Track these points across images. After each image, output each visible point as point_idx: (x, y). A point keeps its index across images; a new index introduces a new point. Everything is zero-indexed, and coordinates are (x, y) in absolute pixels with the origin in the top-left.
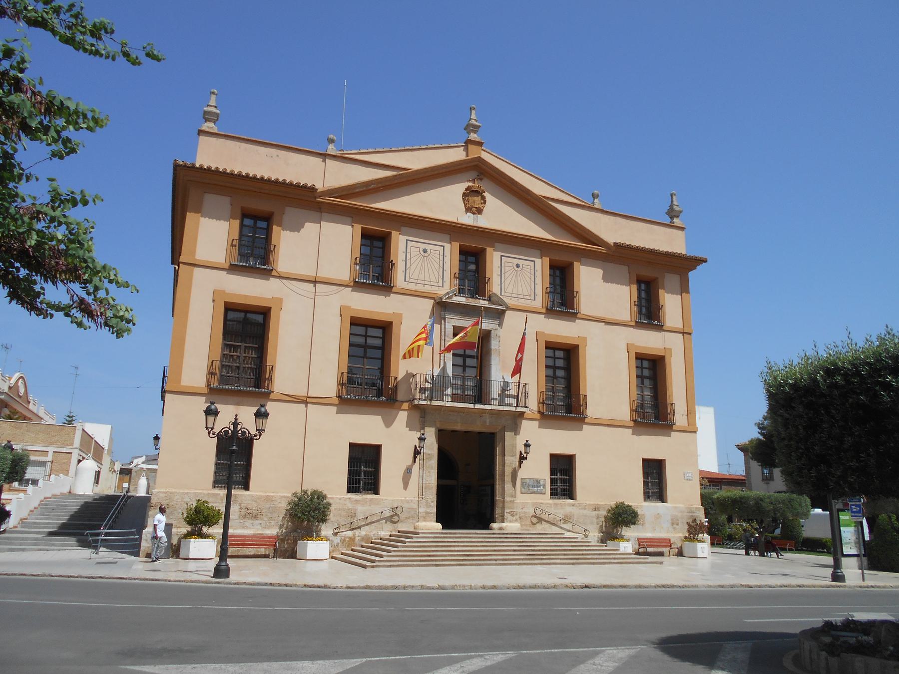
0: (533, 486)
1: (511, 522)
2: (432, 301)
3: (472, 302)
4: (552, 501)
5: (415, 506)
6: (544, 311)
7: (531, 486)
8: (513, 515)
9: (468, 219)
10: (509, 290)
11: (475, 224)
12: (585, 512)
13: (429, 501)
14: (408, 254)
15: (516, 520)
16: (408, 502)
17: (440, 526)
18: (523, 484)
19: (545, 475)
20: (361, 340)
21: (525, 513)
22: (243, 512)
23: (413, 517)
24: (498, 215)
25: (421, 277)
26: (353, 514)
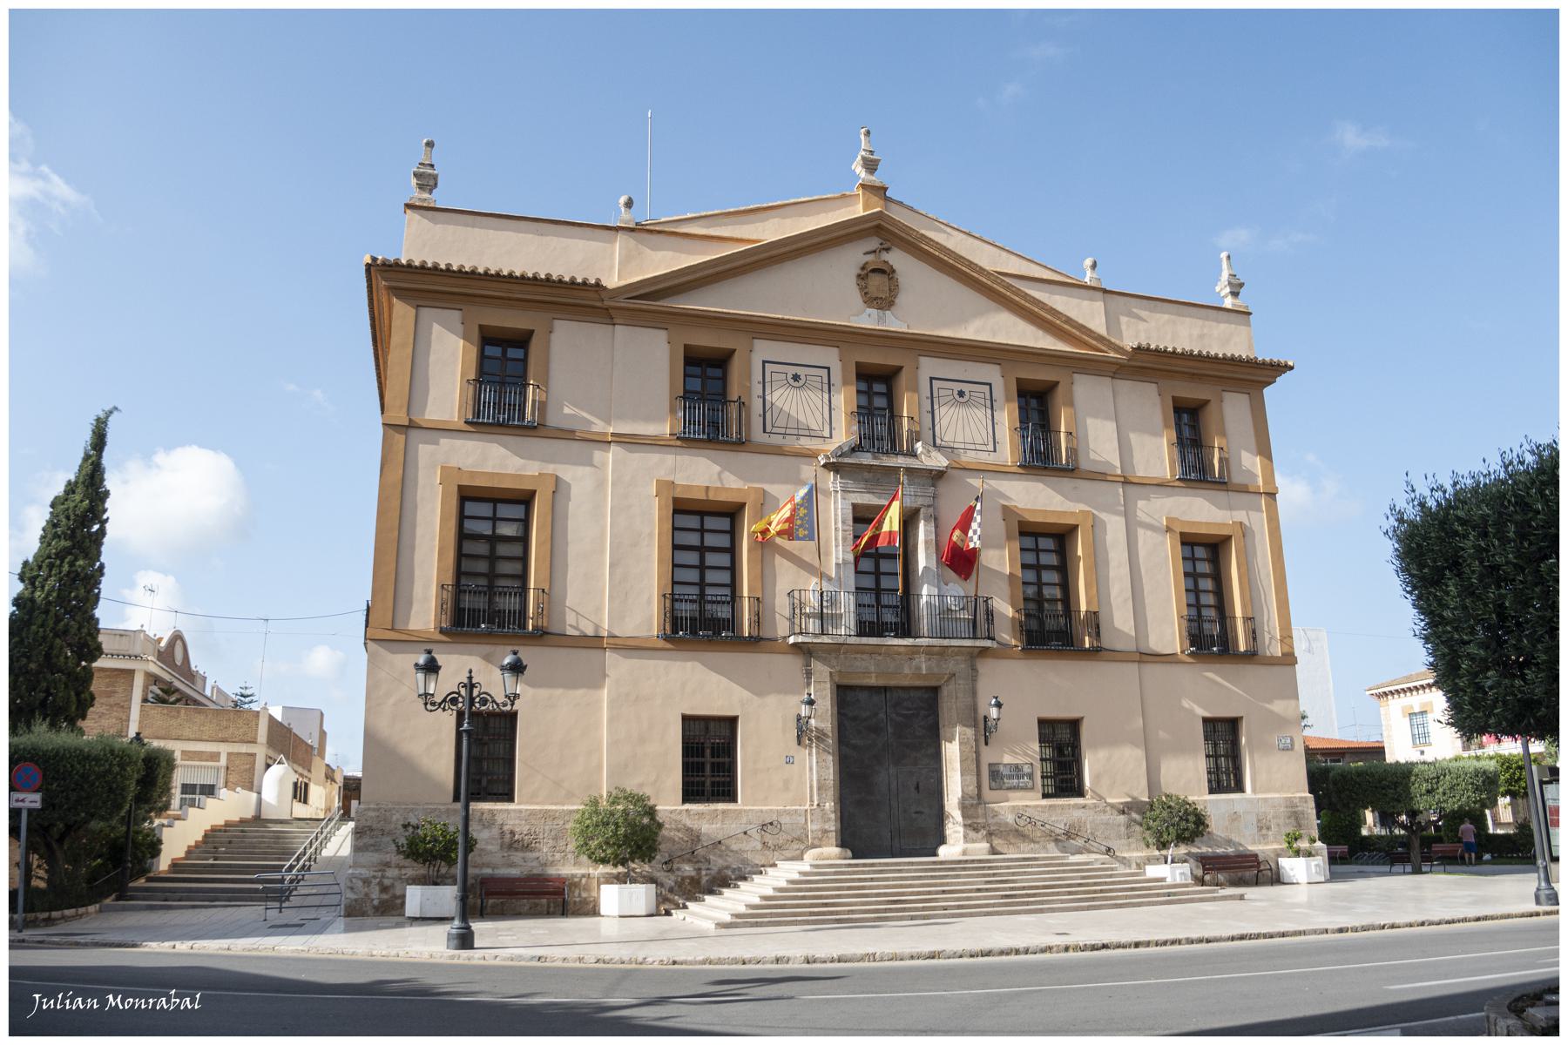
0: (1010, 777)
9: (868, 320)
12: (1105, 817)
20: (693, 539)
24: (926, 306)
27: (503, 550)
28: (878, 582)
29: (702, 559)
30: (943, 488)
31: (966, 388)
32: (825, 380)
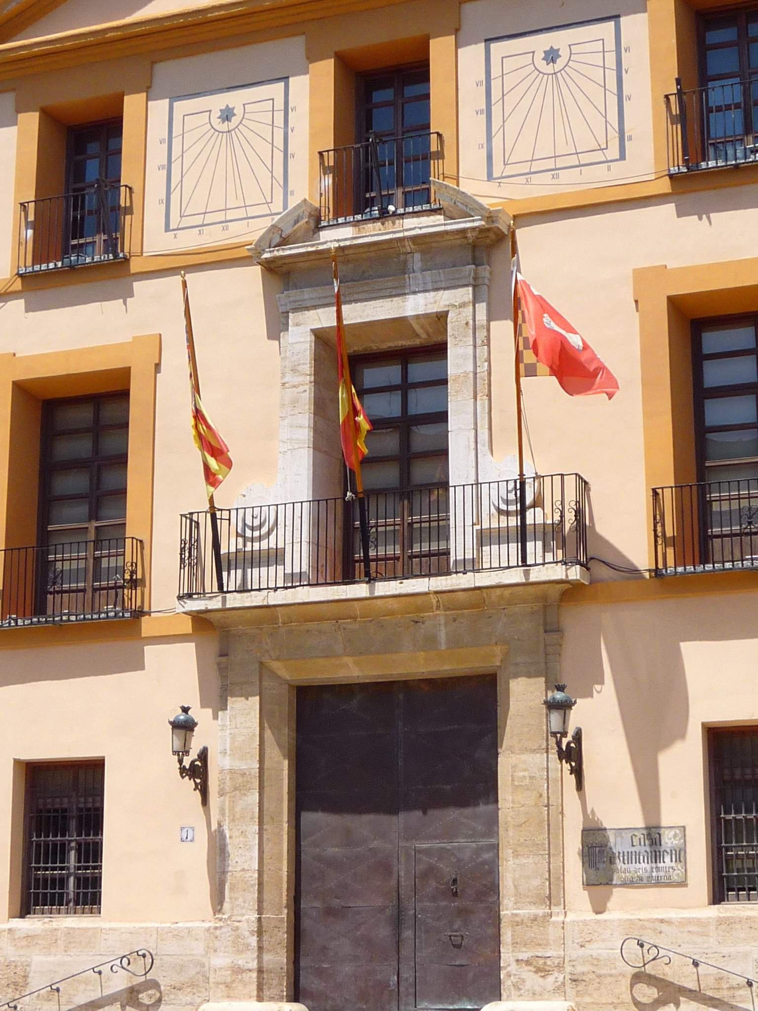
0: (631, 857)
2: (256, 271)
3: (374, 233)
4: (716, 911)
5: (198, 948)
6: (665, 186)
8: (543, 971)
10: (522, 152)
13: (243, 926)
14: (176, 143)
16: (177, 935)
21: (596, 961)
23: (193, 985)
32: (280, 104)
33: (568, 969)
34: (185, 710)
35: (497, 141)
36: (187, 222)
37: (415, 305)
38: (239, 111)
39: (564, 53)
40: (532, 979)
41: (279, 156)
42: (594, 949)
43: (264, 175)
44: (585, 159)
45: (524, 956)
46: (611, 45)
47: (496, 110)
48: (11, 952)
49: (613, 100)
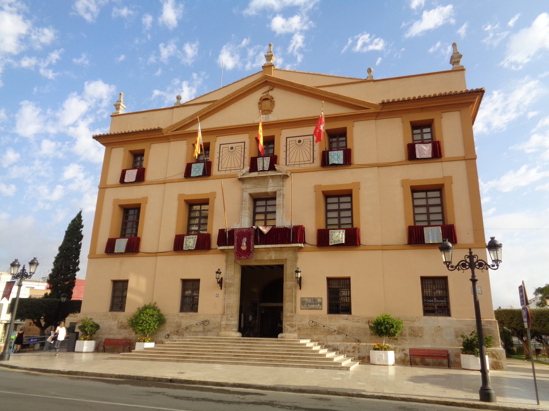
0: (311, 304)
1: (290, 332)
5: (219, 320)
7: (313, 303)
8: (292, 327)
11: (267, 121)
14: (221, 153)
15: (295, 331)
17: (239, 334)
18: (303, 302)
19: (322, 294)
20: (423, 202)
21: (303, 325)
22: (119, 325)
25: (302, 160)
26: (179, 326)
27: (343, 214)
28: (428, 217)
29: (428, 210)
30: (288, 182)
31: (233, 145)
33: (297, 326)
34: (219, 269)
35: (288, 158)
36: (223, 169)
37: (270, 189)
38: (234, 148)
39: (302, 141)
40: (290, 328)
41: (243, 158)
42: (303, 323)
43: (239, 161)
44: (306, 162)
45: (288, 324)
46: (312, 140)
47: (288, 152)
48: (177, 319)
49: (312, 151)
